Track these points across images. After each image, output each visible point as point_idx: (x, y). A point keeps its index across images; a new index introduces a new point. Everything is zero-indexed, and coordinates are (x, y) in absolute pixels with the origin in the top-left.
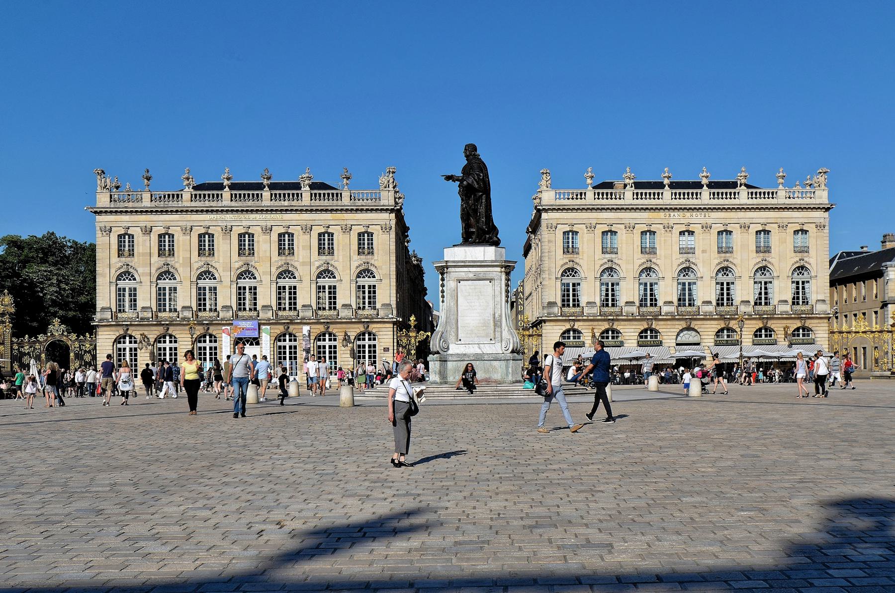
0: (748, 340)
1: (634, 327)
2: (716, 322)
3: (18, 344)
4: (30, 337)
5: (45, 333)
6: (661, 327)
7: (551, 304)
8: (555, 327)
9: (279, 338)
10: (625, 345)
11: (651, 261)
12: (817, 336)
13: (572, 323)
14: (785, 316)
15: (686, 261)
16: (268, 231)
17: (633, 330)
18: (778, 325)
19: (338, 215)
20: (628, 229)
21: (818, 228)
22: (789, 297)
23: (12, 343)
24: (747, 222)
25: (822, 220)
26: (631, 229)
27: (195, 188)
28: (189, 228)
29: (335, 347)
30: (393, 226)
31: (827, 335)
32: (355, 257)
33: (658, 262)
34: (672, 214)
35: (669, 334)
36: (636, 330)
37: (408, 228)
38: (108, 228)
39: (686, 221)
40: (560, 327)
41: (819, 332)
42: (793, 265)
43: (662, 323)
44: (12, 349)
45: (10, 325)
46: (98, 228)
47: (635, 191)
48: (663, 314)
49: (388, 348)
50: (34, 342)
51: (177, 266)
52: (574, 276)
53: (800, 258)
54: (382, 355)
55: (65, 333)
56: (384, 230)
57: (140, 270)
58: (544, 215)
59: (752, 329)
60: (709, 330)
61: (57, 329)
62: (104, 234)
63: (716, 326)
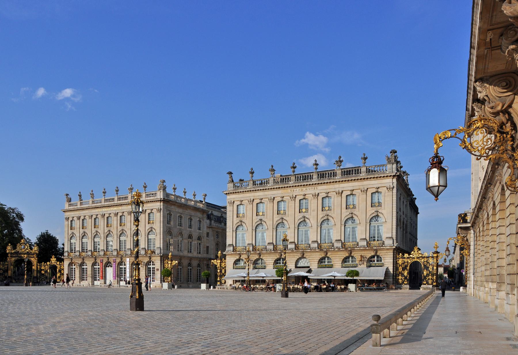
0: (339, 264)
1: (272, 257)
2: (319, 254)
3: (40, 266)
4: (44, 263)
5: (50, 262)
8: (231, 258)
9: (277, 262)
10: (267, 268)
14: (362, 249)
17: (271, 259)
18: (357, 255)
21: (388, 190)
23: (37, 265)
34: (295, 190)
36: (272, 259)
39: (303, 193)
40: (233, 258)
41: (387, 258)
44: (37, 268)
49: (158, 269)
52: (306, 226)
53: (376, 210)
60: (314, 258)
61: (53, 260)
63: (319, 256)
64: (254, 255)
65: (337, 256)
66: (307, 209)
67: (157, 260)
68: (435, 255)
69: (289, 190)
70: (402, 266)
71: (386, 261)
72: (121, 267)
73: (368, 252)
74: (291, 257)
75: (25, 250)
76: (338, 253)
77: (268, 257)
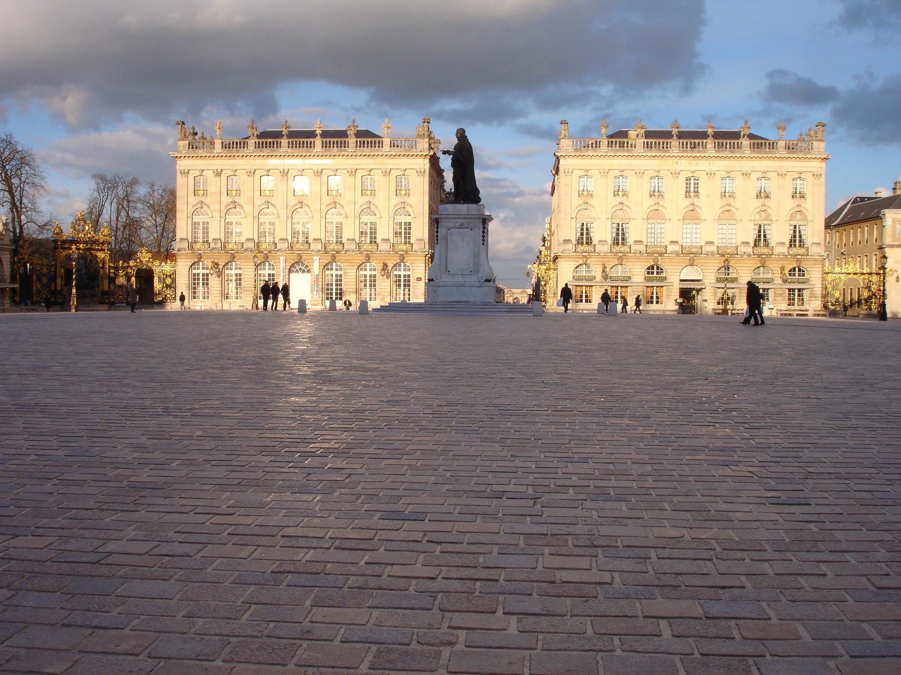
1: (642, 264)
2: (717, 261)
6: (667, 264)
7: (566, 241)
8: (569, 263)
11: (658, 204)
12: (812, 276)
13: (585, 260)
15: (691, 204)
16: (319, 174)
17: (640, 267)
18: (776, 265)
19: (380, 160)
20: (638, 174)
22: (786, 239)
24: (749, 169)
25: (819, 170)
26: (641, 174)
27: (259, 137)
28: (253, 170)
29: (375, 276)
30: (427, 171)
31: (820, 276)
32: (393, 197)
33: (665, 205)
34: (679, 162)
35: (674, 271)
37: (443, 171)
38: (186, 171)
41: (814, 272)
42: (791, 210)
43: (667, 260)
45: (109, 252)
46: (178, 171)
47: (646, 141)
48: (668, 252)
49: (421, 278)
50: (127, 267)
51: (242, 203)
54: (415, 284)
55: (151, 260)
56: (419, 173)
57: (212, 207)
58: (562, 162)
59: (751, 269)
62: (184, 176)
63: (715, 265)
64: (610, 260)
65: (745, 265)
66: (696, 192)
67: (416, 262)
68: (882, 272)
69: (670, 161)
70: (831, 284)
71: (812, 276)
72: (363, 273)
73: (788, 262)
74: (673, 264)
75: (84, 234)
76: (747, 262)
77: (636, 263)
